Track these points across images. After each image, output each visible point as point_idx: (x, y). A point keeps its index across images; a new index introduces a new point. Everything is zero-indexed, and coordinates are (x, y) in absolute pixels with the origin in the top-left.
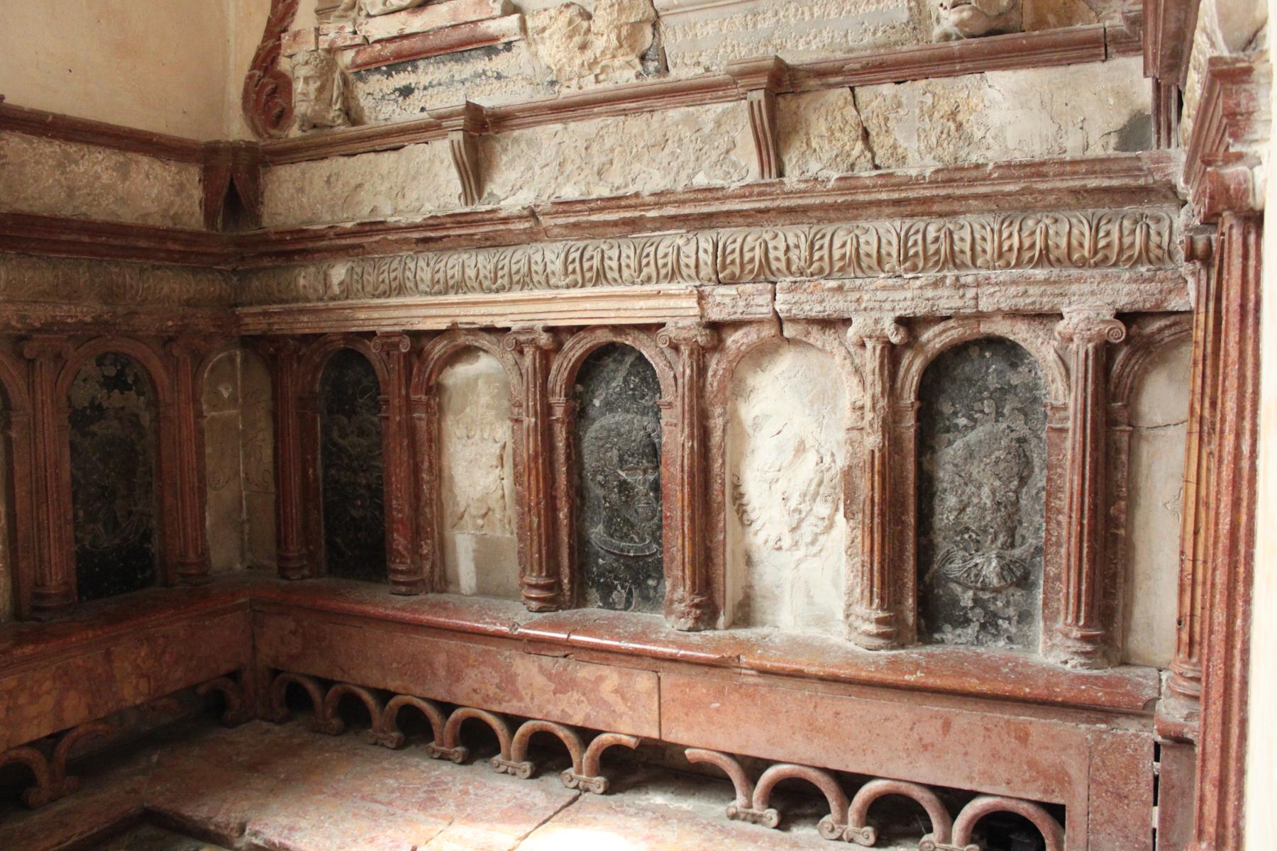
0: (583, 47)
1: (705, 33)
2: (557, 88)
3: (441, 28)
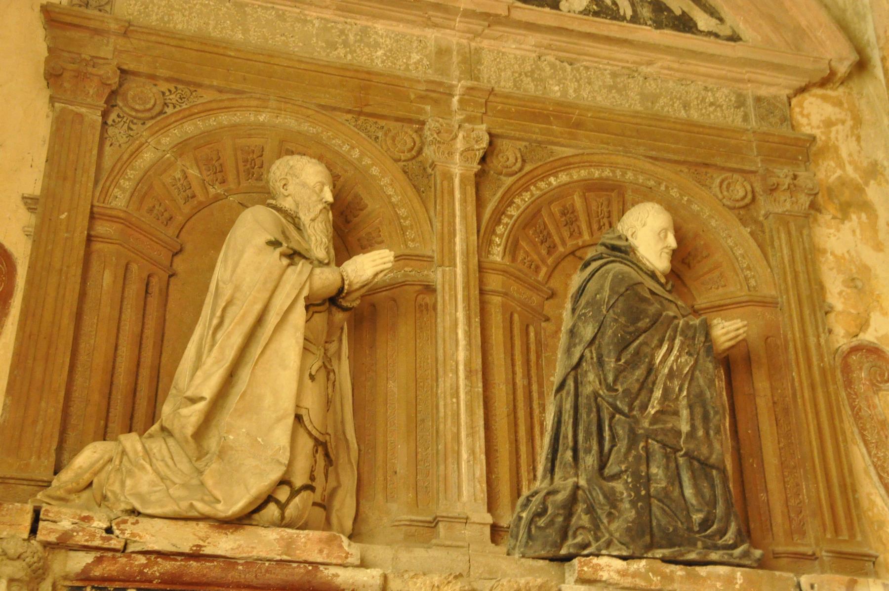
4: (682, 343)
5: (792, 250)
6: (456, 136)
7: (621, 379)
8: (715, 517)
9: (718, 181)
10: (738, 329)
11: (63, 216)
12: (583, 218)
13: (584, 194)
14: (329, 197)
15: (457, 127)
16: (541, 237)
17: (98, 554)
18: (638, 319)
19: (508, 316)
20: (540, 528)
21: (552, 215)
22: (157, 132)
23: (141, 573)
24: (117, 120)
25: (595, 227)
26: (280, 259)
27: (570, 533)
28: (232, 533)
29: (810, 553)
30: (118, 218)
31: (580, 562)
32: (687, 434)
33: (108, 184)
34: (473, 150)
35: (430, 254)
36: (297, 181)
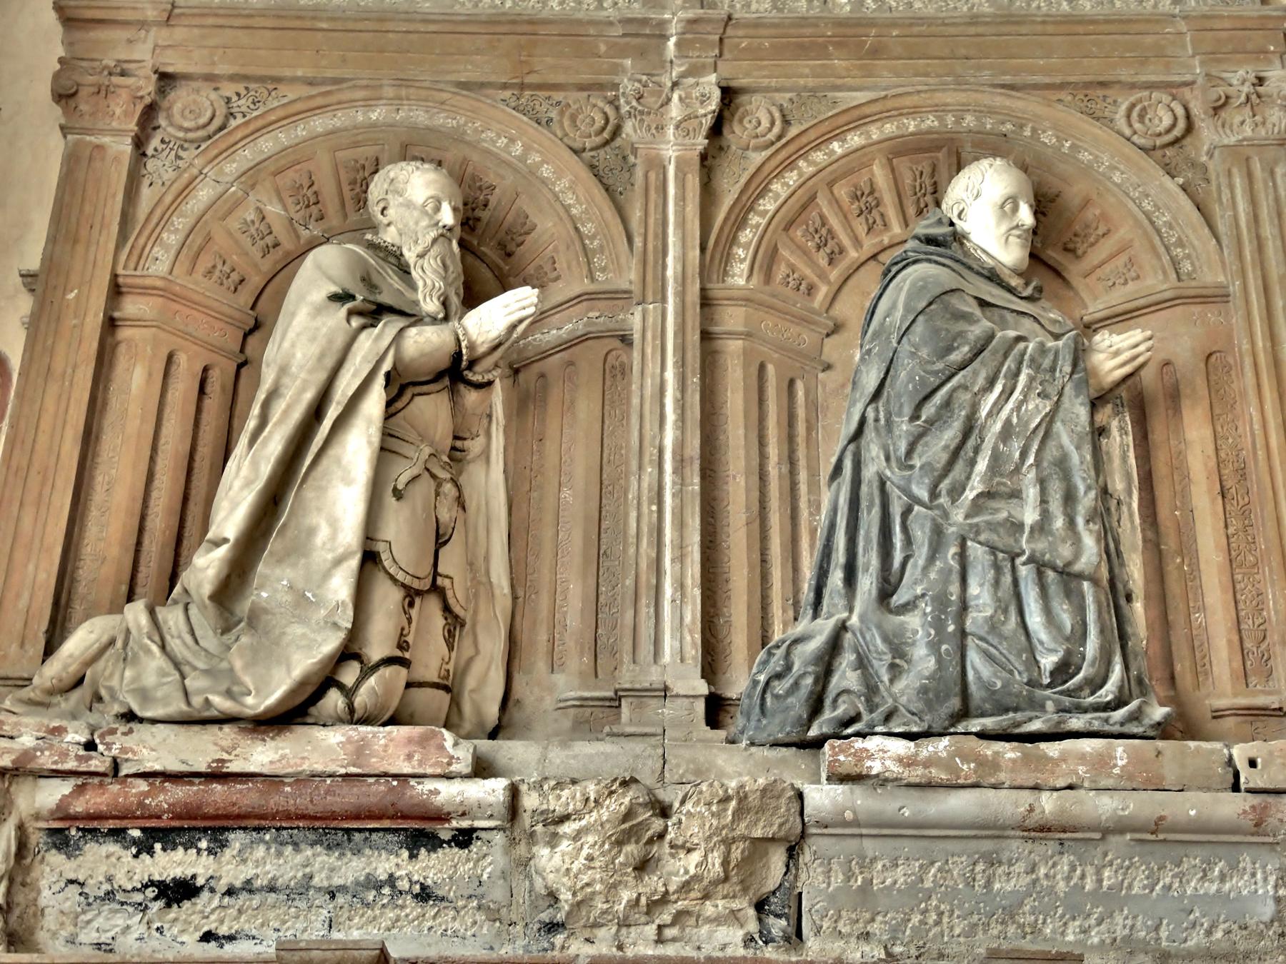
0: (643, 866)
1: (889, 882)
2: (559, 939)
3: (322, 775)
4: (1031, 379)
5: (1253, 202)
6: (669, 100)
7: (919, 448)
8: (1084, 658)
9: (1124, 107)
10: (1136, 346)
11: (71, 296)
12: (889, 199)
13: (890, 160)
14: (447, 216)
15: (669, 84)
16: (817, 239)
17: (80, 781)
18: (949, 349)
19: (754, 370)
20: (777, 697)
21: (836, 202)
22: (216, 157)
23: (141, 804)
24: (160, 147)
25: (911, 211)
26: (348, 321)
27: (828, 702)
28: (272, 738)
29: (1276, 706)
30: (154, 288)
31: (833, 747)
32: (1032, 528)
33: (142, 241)
34: (697, 117)
35: (625, 286)
36: (401, 200)
